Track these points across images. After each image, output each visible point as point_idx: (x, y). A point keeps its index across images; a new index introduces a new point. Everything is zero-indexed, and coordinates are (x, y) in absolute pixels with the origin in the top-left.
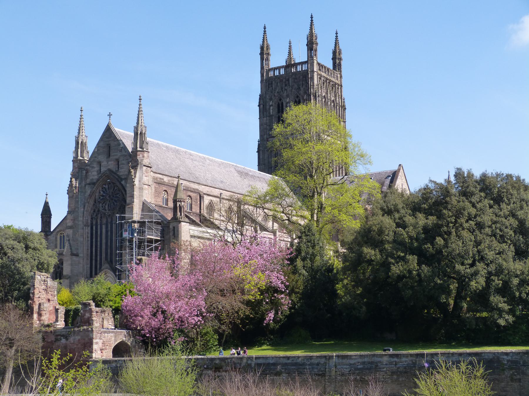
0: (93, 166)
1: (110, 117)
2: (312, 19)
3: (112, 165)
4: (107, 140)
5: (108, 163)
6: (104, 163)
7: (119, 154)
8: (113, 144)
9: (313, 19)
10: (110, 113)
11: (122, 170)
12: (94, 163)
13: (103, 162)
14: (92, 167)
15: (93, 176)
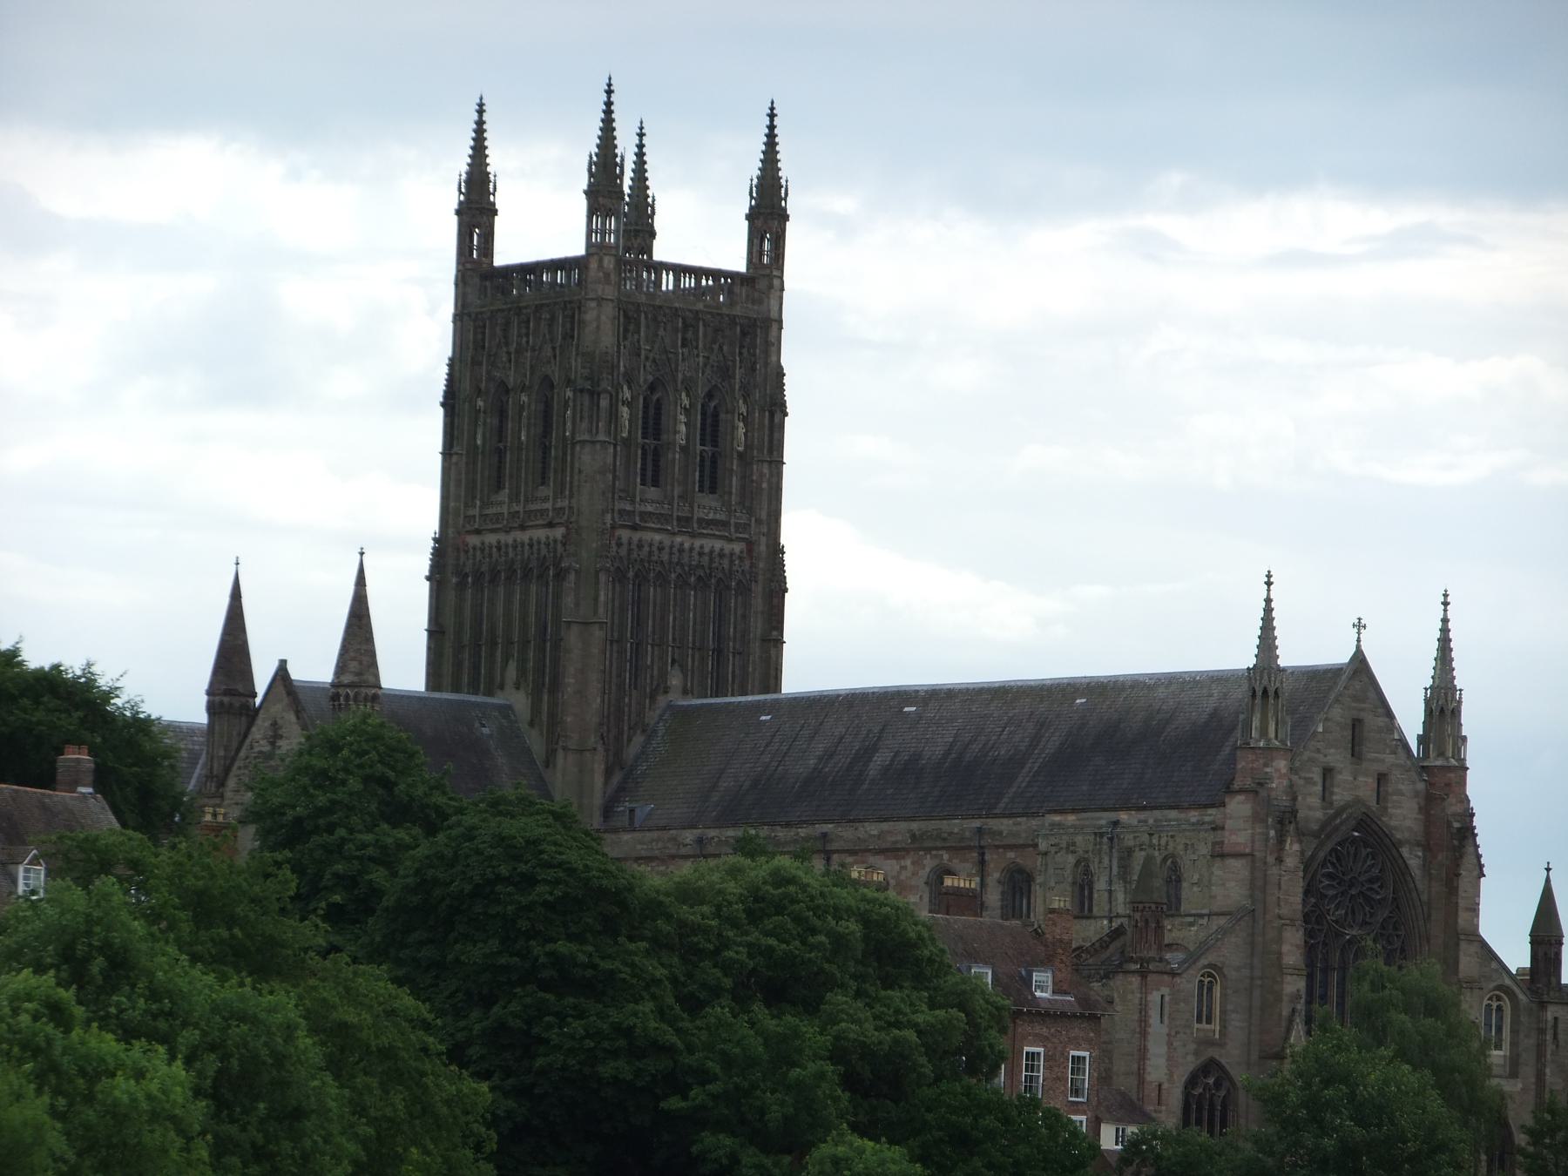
0: (1312, 778)
1: (1359, 633)
2: (609, 97)
3: (1366, 788)
4: (1354, 705)
5: (1355, 779)
6: (1344, 776)
7: (1390, 759)
8: (1372, 721)
9: (614, 98)
10: (1359, 619)
11: (1399, 811)
12: (1314, 769)
13: (1340, 773)
14: (1305, 778)
15: (1310, 808)
